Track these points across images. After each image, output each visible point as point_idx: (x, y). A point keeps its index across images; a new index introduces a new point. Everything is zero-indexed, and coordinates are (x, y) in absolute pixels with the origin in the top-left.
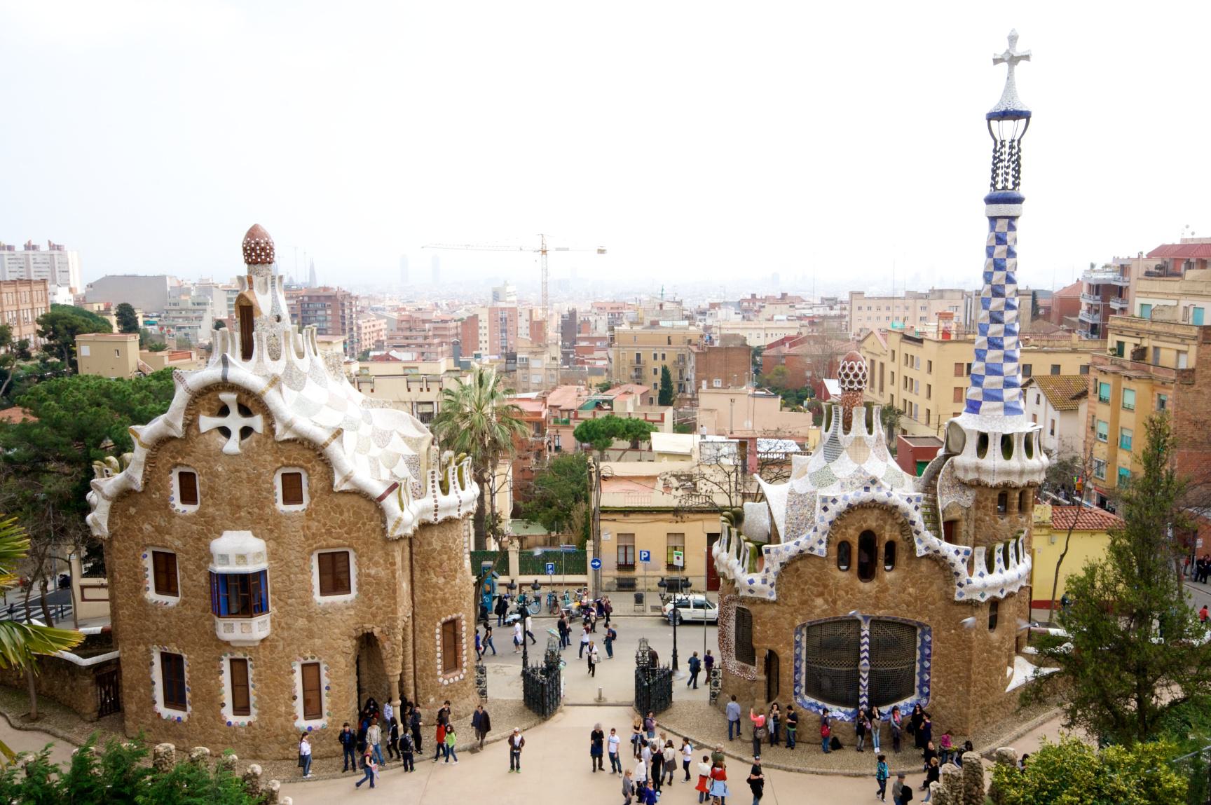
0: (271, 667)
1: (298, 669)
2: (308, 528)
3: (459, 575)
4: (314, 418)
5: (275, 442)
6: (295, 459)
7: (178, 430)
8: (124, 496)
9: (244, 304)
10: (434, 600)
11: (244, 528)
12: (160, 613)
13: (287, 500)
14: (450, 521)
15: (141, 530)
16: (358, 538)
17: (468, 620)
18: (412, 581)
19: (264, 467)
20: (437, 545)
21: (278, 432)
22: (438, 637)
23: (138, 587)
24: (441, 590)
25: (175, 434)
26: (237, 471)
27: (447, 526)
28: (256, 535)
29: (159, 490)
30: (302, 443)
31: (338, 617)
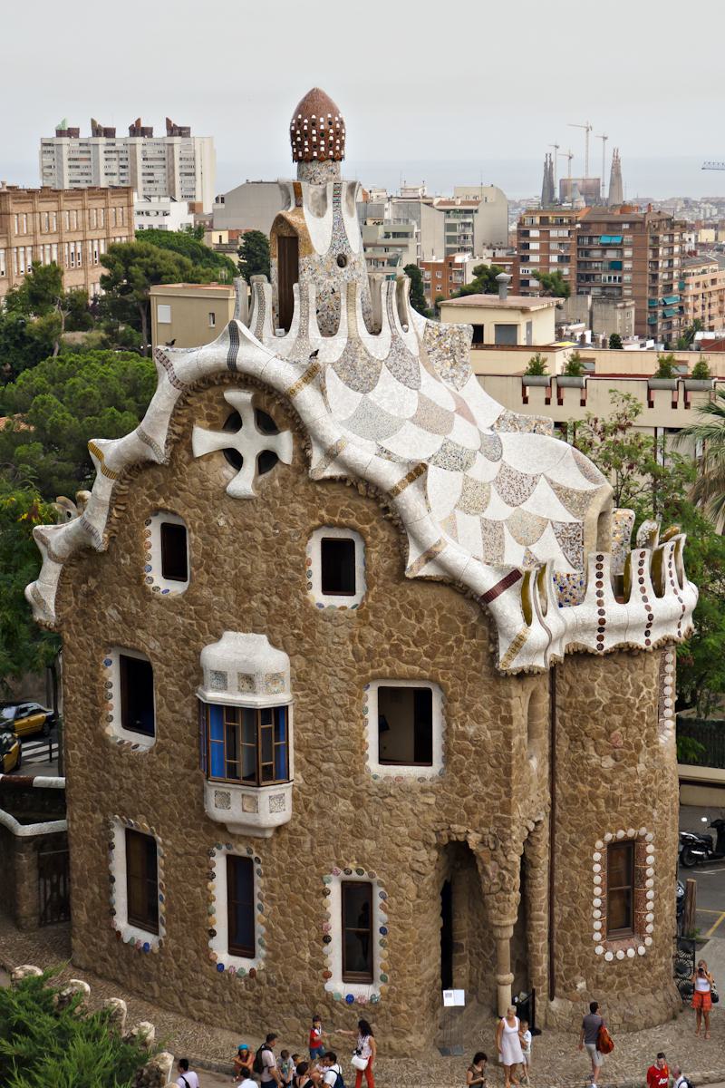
0: (291, 879)
1: (335, 889)
3: (644, 757)
4: (385, 444)
5: (311, 481)
6: (344, 514)
7: (160, 453)
8: (82, 556)
9: (286, 233)
10: (593, 797)
11: (256, 629)
12: (125, 761)
13: (330, 587)
14: (628, 652)
15: (103, 615)
16: (447, 666)
17: (659, 843)
18: (552, 757)
20: (602, 695)
21: (314, 464)
22: (597, 868)
23: (97, 716)
24: (607, 780)
25: (154, 457)
26: (249, 527)
27: (624, 661)
28: (274, 643)
29: (129, 551)
30: (354, 487)
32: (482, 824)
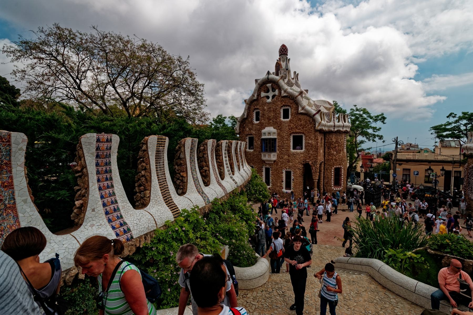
1: (284, 172)
2: (290, 126)
3: (342, 153)
7: (255, 97)
10: (332, 159)
11: (271, 126)
13: (284, 118)
14: (339, 132)
16: (306, 130)
17: (344, 169)
18: (324, 152)
19: (278, 106)
20: (334, 140)
26: (270, 108)
27: (338, 134)
28: (274, 128)
30: (289, 98)
31: (298, 156)
32: (312, 160)
